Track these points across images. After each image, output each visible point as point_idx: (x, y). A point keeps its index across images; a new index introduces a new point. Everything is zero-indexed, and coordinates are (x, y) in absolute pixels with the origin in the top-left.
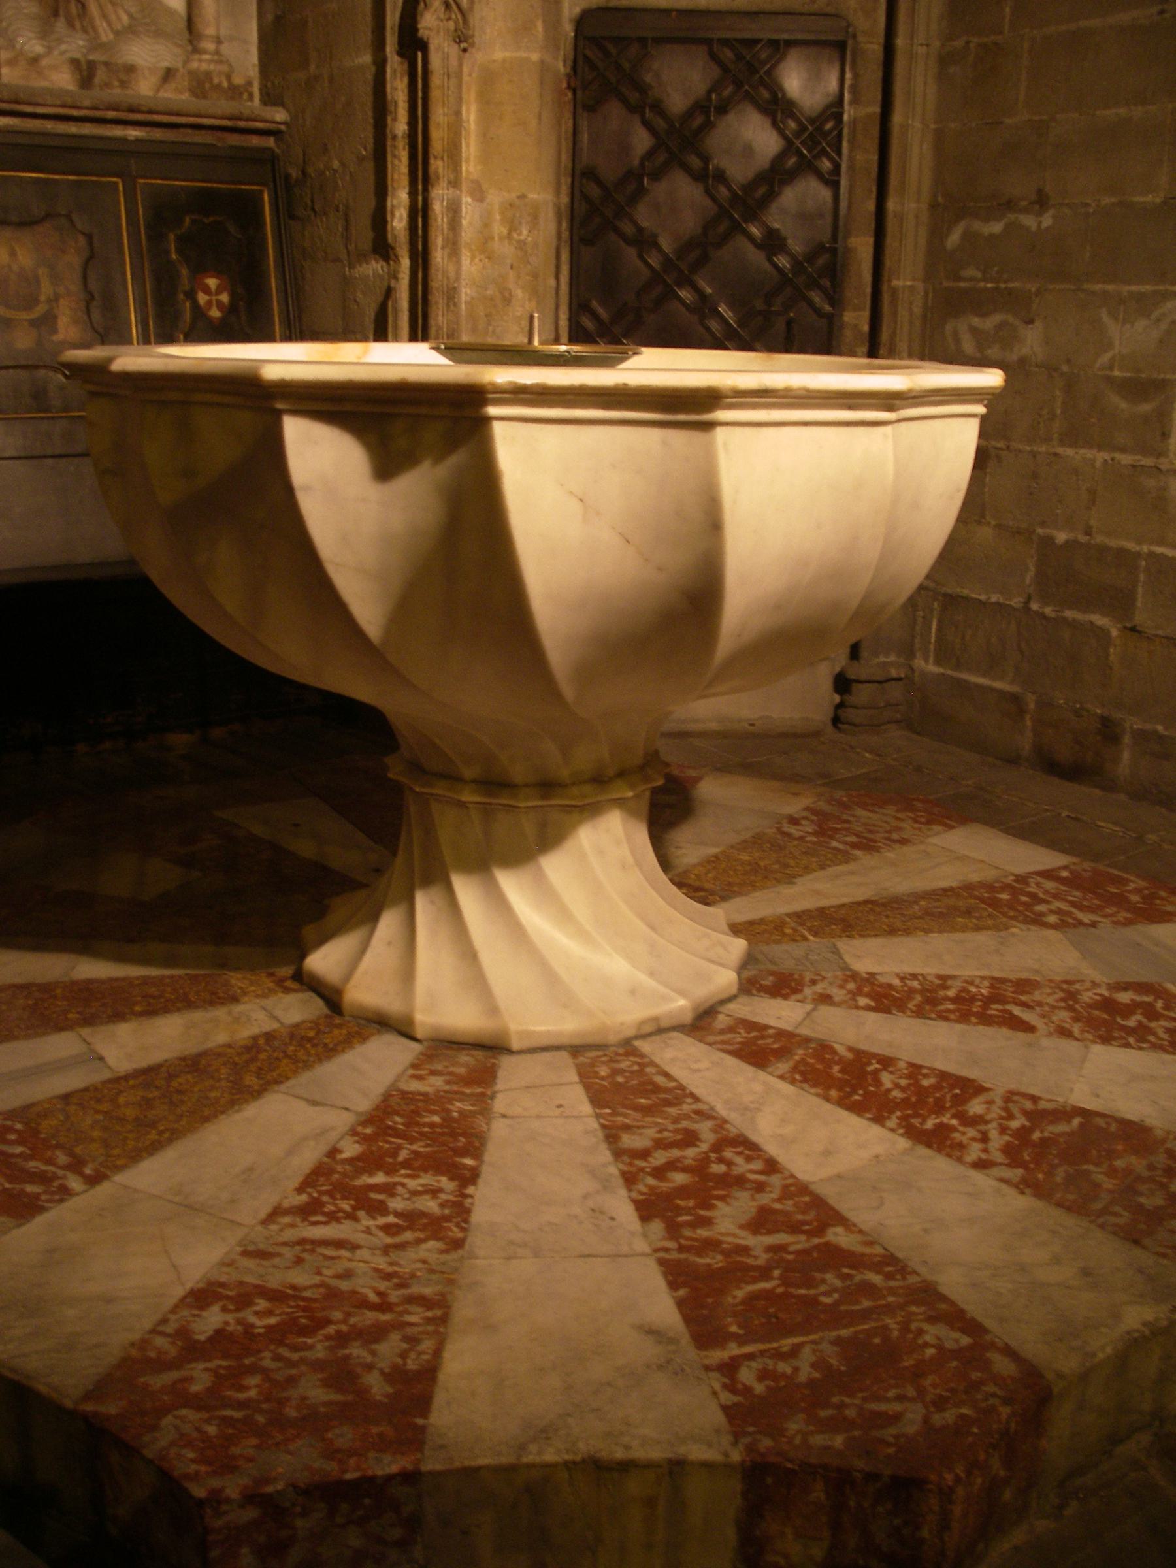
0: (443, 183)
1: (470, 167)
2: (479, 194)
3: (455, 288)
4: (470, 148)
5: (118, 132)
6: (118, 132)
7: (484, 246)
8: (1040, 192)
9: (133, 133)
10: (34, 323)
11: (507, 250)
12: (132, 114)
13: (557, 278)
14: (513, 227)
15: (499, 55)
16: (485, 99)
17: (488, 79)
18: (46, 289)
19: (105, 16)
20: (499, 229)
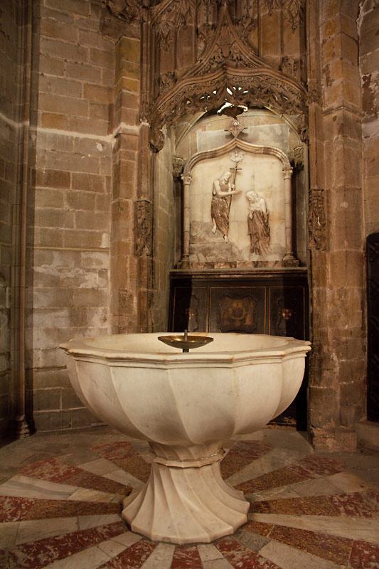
0: (315, 286)
1: (329, 281)
2: (331, 288)
3: (48, 335)
4: (329, 276)
5: (266, 276)
6: (266, 276)
7: (333, 302)
8: (105, 317)
9: (270, 276)
10: (241, 320)
11: (338, 303)
12: (270, 272)
13: (363, 309)
14: (340, 297)
15: (335, 251)
16: (332, 263)
17: (333, 257)
18: (244, 312)
19: (264, 251)
20: (337, 297)
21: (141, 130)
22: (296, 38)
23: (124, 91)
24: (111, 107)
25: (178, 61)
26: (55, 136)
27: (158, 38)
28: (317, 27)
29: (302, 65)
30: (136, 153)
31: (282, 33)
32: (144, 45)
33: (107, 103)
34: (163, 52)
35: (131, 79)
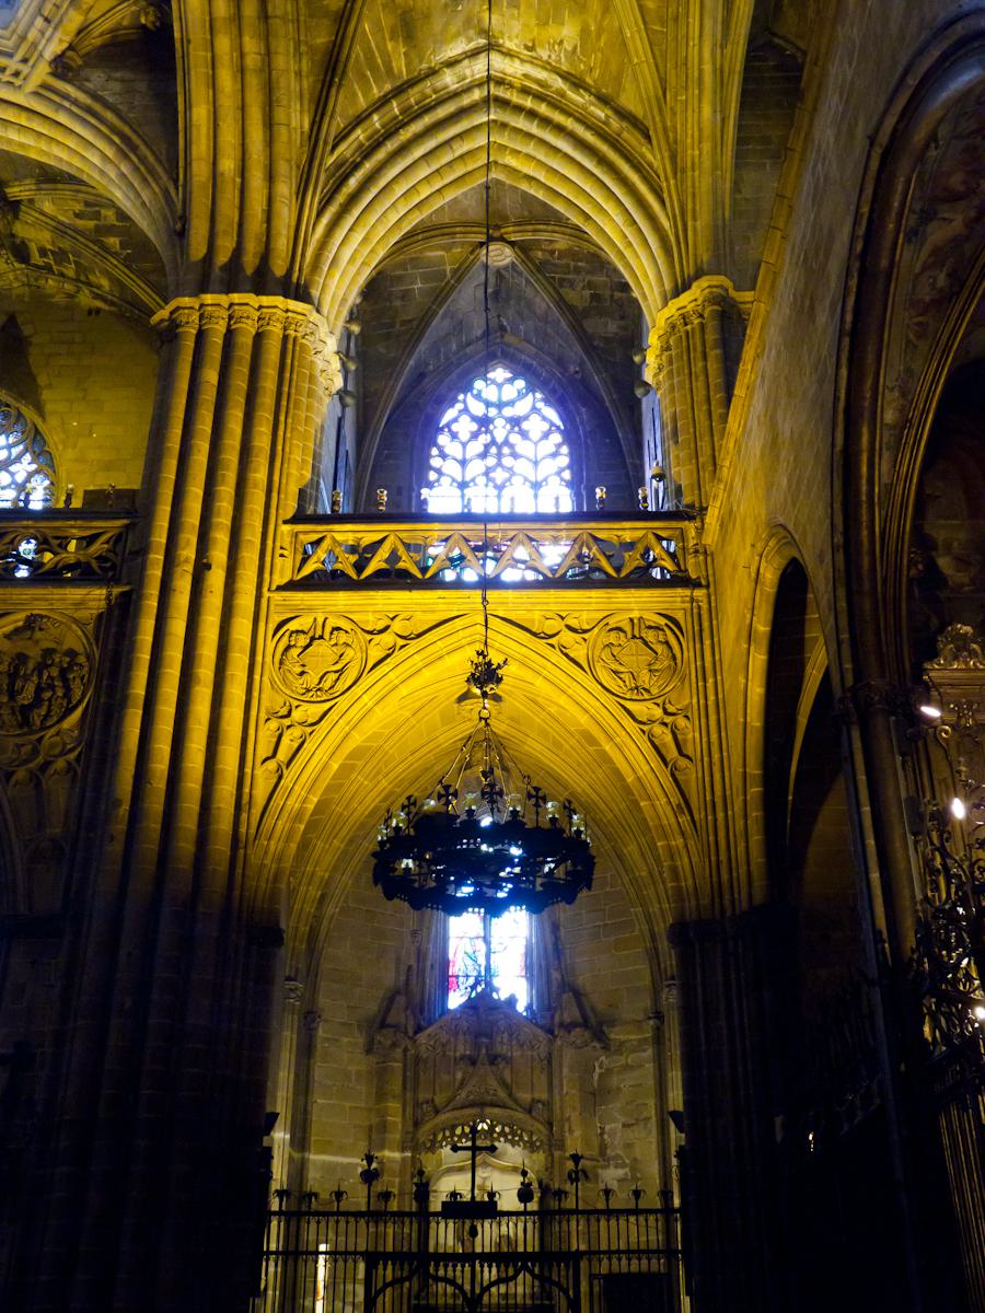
21: (404, 1159)
22: (544, 1078)
23: (389, 1118)
24: (370, 1128)
25: (437, 1086)
26: (324, 1162)
27: (417, 1060)
28: (561, 1081)
29: (548, 1105)
30: (397, 1180)
31: (532, 1073)
32: (408, 1074)
33: (367, 1124)
34: (422, 1074)
35: (394, 1106)
